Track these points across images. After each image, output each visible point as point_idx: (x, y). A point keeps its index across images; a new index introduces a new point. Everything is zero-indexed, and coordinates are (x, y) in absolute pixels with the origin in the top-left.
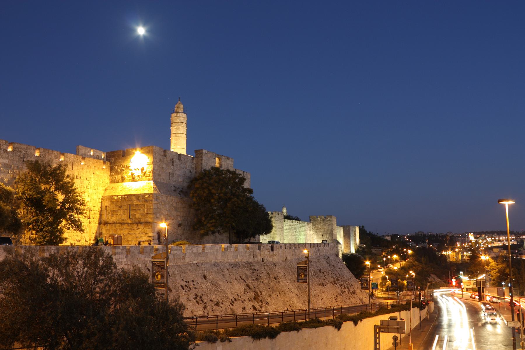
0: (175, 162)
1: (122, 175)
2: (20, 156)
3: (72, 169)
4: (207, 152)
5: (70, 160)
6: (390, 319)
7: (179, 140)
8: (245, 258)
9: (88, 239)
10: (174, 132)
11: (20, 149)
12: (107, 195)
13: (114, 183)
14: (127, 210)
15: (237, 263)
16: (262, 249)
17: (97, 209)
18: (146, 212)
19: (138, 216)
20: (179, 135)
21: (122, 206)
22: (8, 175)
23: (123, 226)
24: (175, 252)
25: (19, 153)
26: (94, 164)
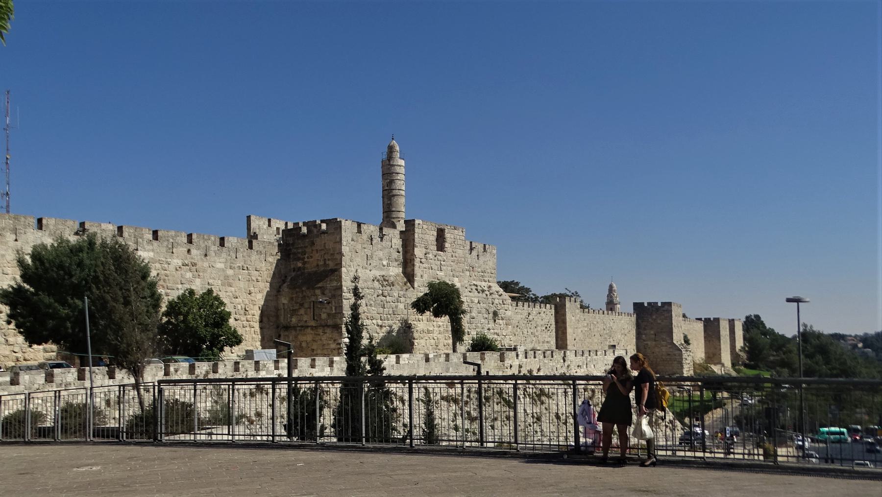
0: (374, 239)
3: (236, 258)
4: (421, 222)
7: (394, 198)
10: (387, 188)
14: (310, 308)
18: (334, 312)
19: (324, 316)
20: (395, 192)
21: (303, 303)
26: (264, 247)
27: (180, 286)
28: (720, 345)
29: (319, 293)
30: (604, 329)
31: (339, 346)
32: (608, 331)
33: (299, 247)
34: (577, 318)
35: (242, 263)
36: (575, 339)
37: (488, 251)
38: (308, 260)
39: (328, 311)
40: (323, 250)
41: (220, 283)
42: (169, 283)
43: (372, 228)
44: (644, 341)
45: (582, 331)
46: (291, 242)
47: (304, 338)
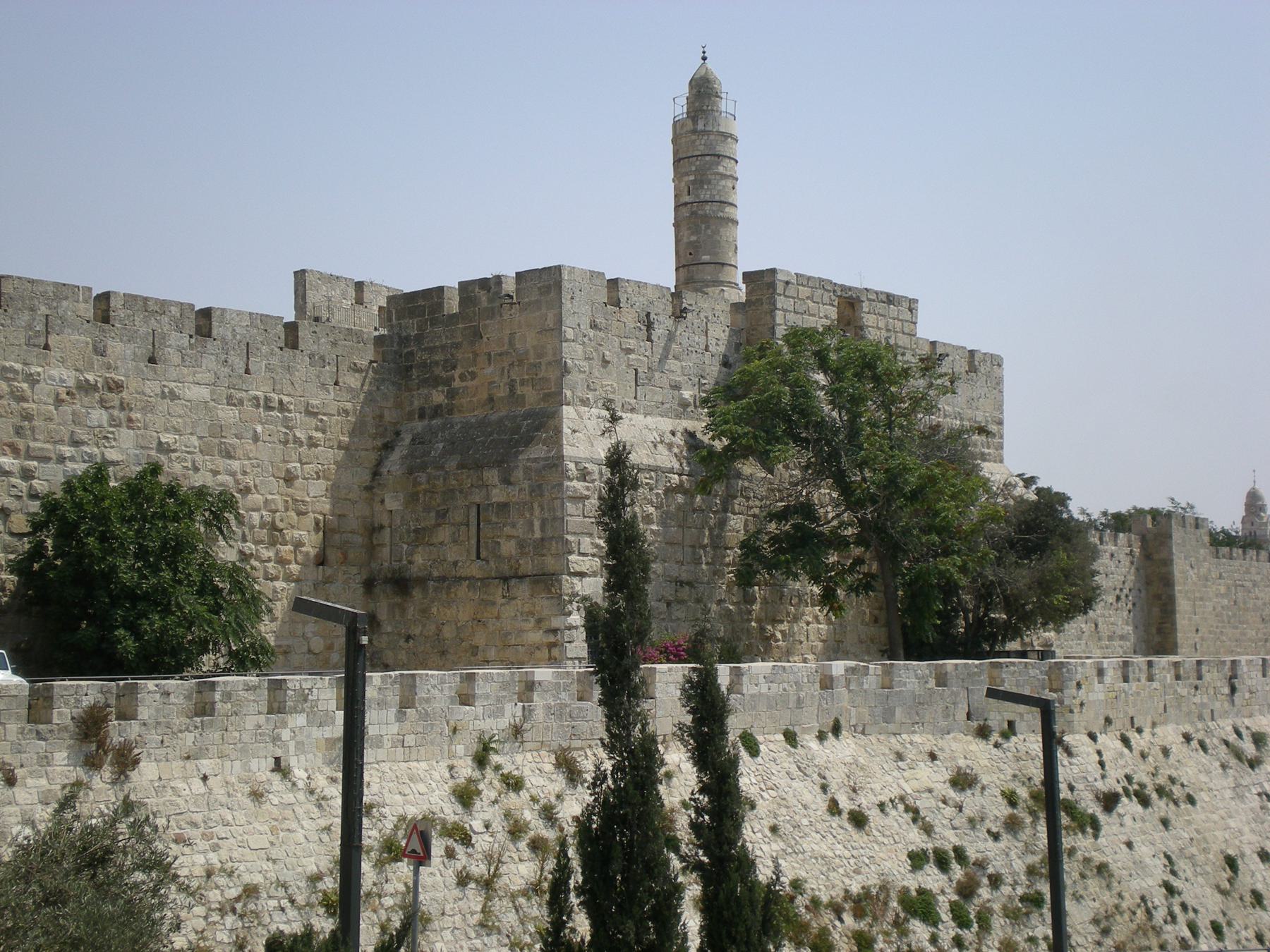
2: (30, 327)
3: (247, 371)
5: (234, 336)
7: (707, 228)
10: (687, 199)
11: (32, 298)
14: (468, 525)
18: (538, 535)
19: (508, 548)
20: (707, 207)
26: (334, 344)
27: (67, 451)
29: (496, 481)
31: (552, 639)
33: (435, 347)
34: (1203, 571)
36: (1197, 630)
37: (982, 370)
38: (464, 384)
39: (520, 532)
40: (507, 353)
41: (197, 444)
42: (35, 440)
46: (412, 334)
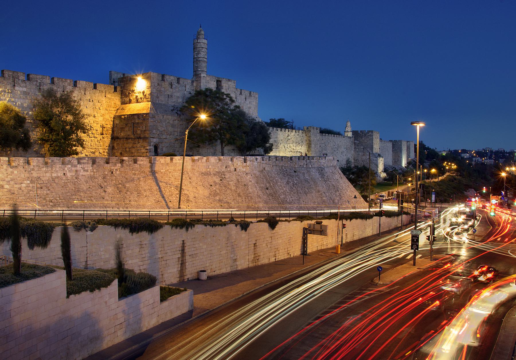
0: (173, 85)
1: (129, 97)
2: (36, 85)
3: (85, 94)
4: (205, 76)
6: (317, 223)
8: (217, 168)
9: (101, 151)
10: (196, 57)
11: (36, 79)
12: (117, 114)
13: (124, 104)
14: (131, 127)
15: (209, 172)
16: (235, 161)
17: (110, 127)
18: (144, 129)
19: (139, 132)
22: (27, 101)
23: (128, 140)
24: (142, 163)
25: (35, 83)
26: (105, 89)
28: (401, 155)
30: (334, 145)
32: (336, 147)
34: (318, 139)
35: (89, 98)
43: (172, 78)
44: (357, 152)
45: (320, 146)
47: (128, 145)
